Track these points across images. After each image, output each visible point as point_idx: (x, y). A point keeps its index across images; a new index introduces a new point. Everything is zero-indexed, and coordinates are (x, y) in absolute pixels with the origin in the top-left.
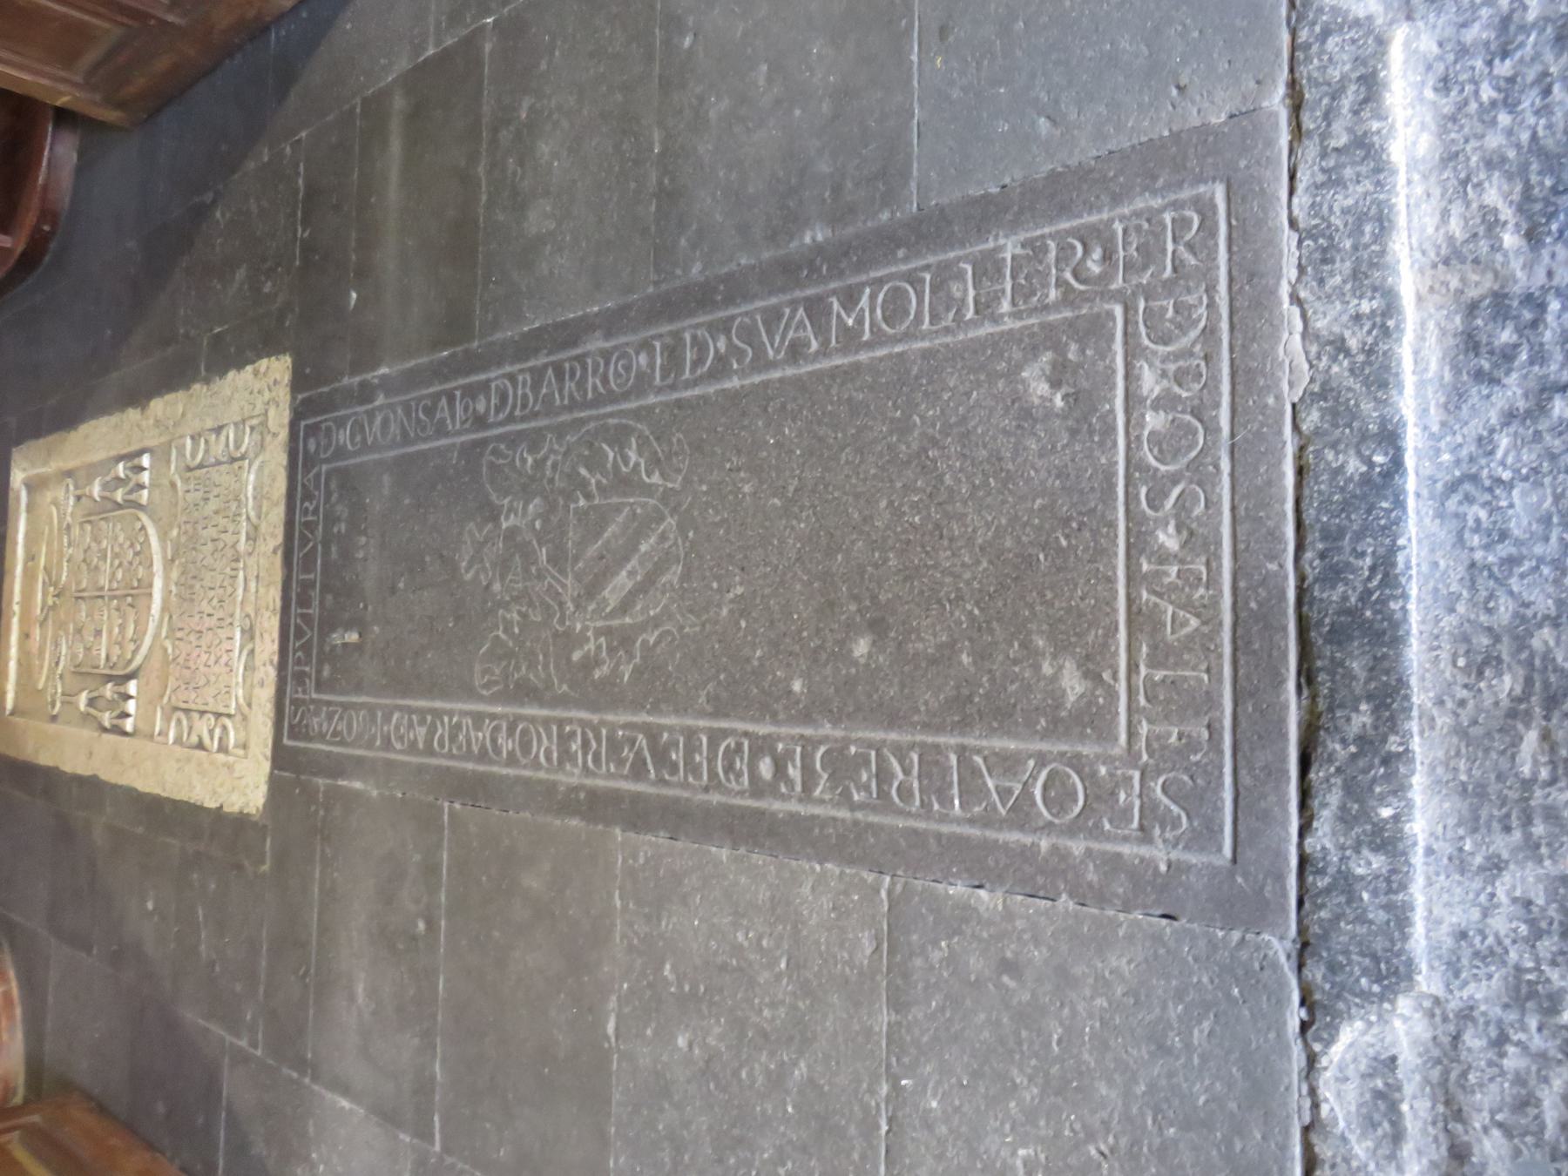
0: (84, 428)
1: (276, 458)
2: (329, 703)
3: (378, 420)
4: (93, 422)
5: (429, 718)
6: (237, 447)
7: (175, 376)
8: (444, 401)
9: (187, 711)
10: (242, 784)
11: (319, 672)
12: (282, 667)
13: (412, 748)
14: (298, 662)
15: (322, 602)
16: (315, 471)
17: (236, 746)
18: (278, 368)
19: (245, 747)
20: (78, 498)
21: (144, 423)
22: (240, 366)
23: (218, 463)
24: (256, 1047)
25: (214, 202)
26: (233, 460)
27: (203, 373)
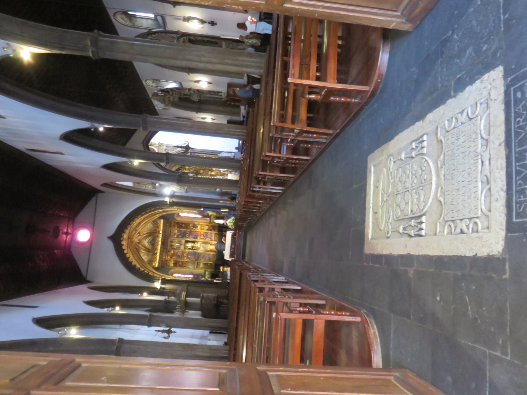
0: (396, 138)
4: (401, 134)
9: (453, 221)
10: (491, 242)
14: (520, 185)
17: (482, 229)
19: (488, 228)
27: (452, 94)
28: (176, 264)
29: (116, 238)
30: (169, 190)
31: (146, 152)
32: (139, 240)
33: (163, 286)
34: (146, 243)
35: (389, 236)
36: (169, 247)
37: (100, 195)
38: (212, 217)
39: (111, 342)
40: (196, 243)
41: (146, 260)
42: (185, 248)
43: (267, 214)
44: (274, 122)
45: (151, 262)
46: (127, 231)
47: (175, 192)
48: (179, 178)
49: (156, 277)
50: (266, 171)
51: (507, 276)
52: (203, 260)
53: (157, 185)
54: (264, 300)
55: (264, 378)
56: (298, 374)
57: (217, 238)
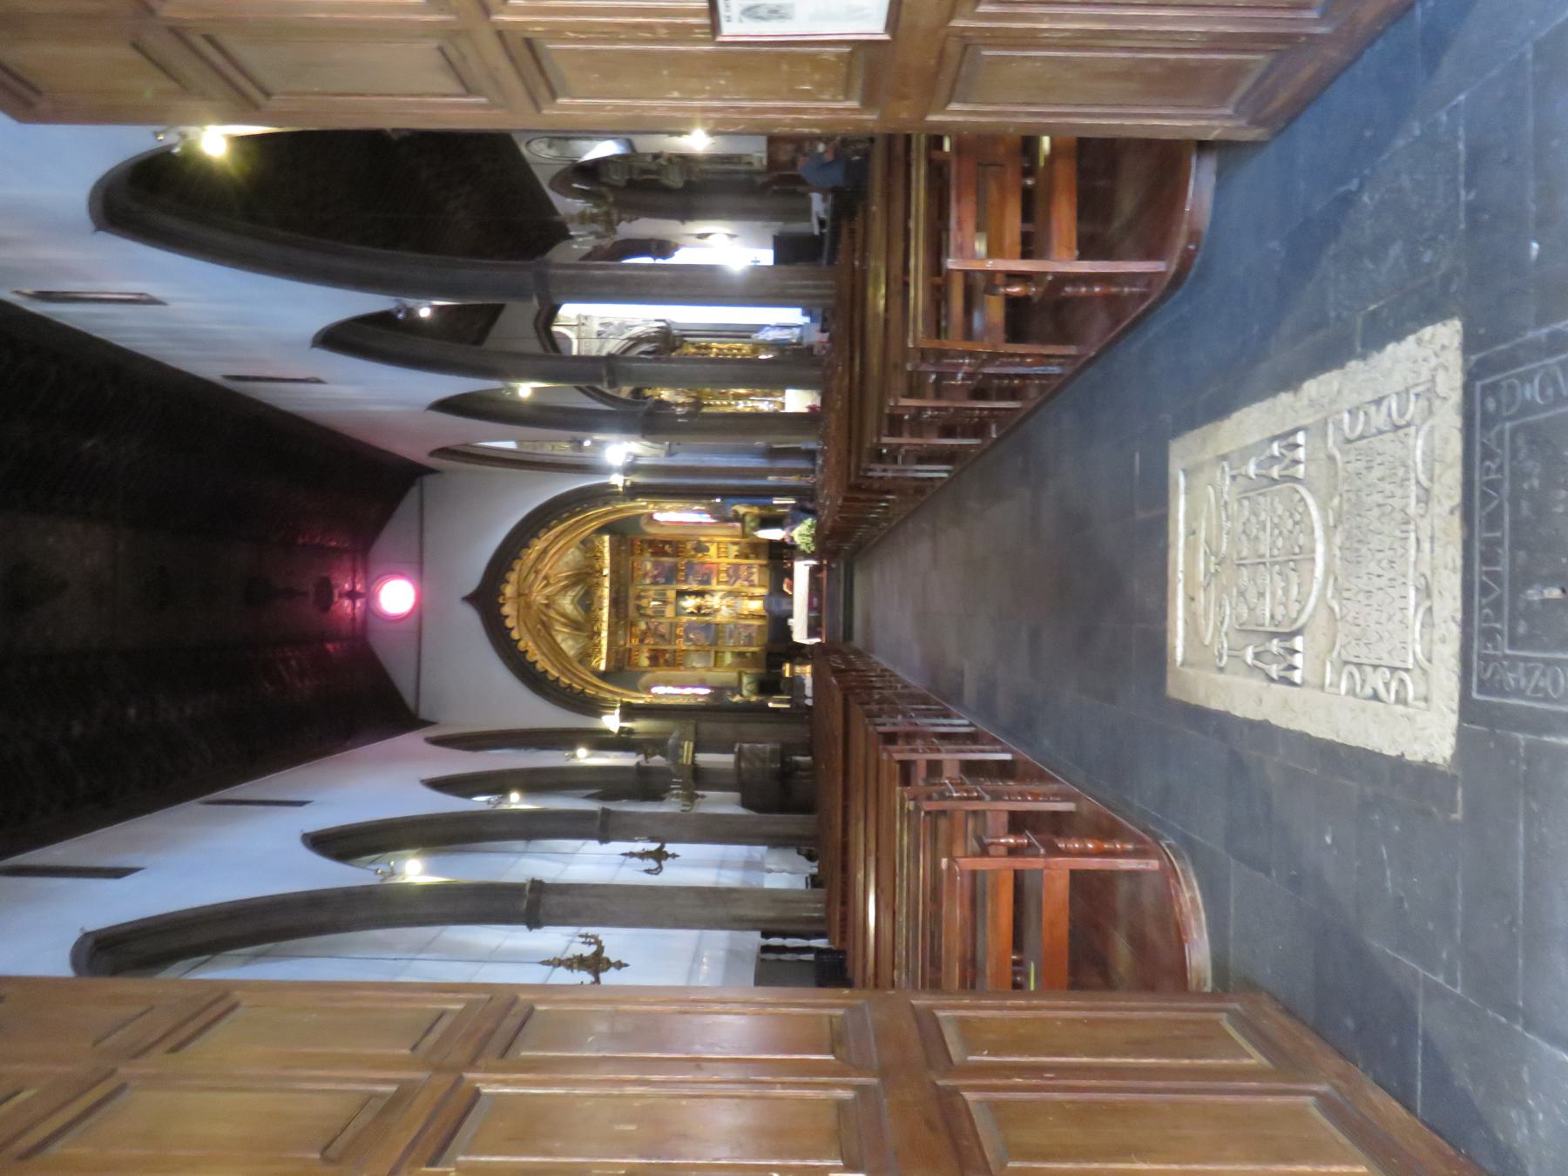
0: (1237, 416)
1: (1449, 420)
2: (1526, 659)
4: (1246, 410)
6: (1401, 415)
7: (1330, 356)
9: (1359, 665)
10: (1427, 732)
11: (1512, 629)
12: (1466, 624)
15: (1513, 560)
16: (1497, 428)
17: (1416, 699)
18: (1446, 335)
19: (1426, 699)
20: (1234, 478)
21: (1298, 405)
22: (1399, 336)
23: (1380, 432)
24: (1455, 986)
25: (1361, 187)
26: (1397, 428)
27: (1359, 349)
28: (655, 658)
29: (486, 599)
30: (619, 453)
31: (551, 357)
32: (547, 598)
33: (627, 725)
34: (567, 603)
35: (1222, 664)
36: (632, 612)
37: (428, 480)
38: (748, 518)
39: (514, 890)
40: (708, 597)
41: (571, 653)
42: (679, 611)
43: (910, 525)
44: (915, 338)
45: (585, 656)
46: (513, 577)
47: (636, 457)
48: (648, 420)
49: (605, 700)
50: (900, 435)
51: (1457, 816)
52: (731, 642)
53: (587, 443)
54: (918, 809)
55: (929, 1028)
56: (1005, 1013)
57: (766, 579)
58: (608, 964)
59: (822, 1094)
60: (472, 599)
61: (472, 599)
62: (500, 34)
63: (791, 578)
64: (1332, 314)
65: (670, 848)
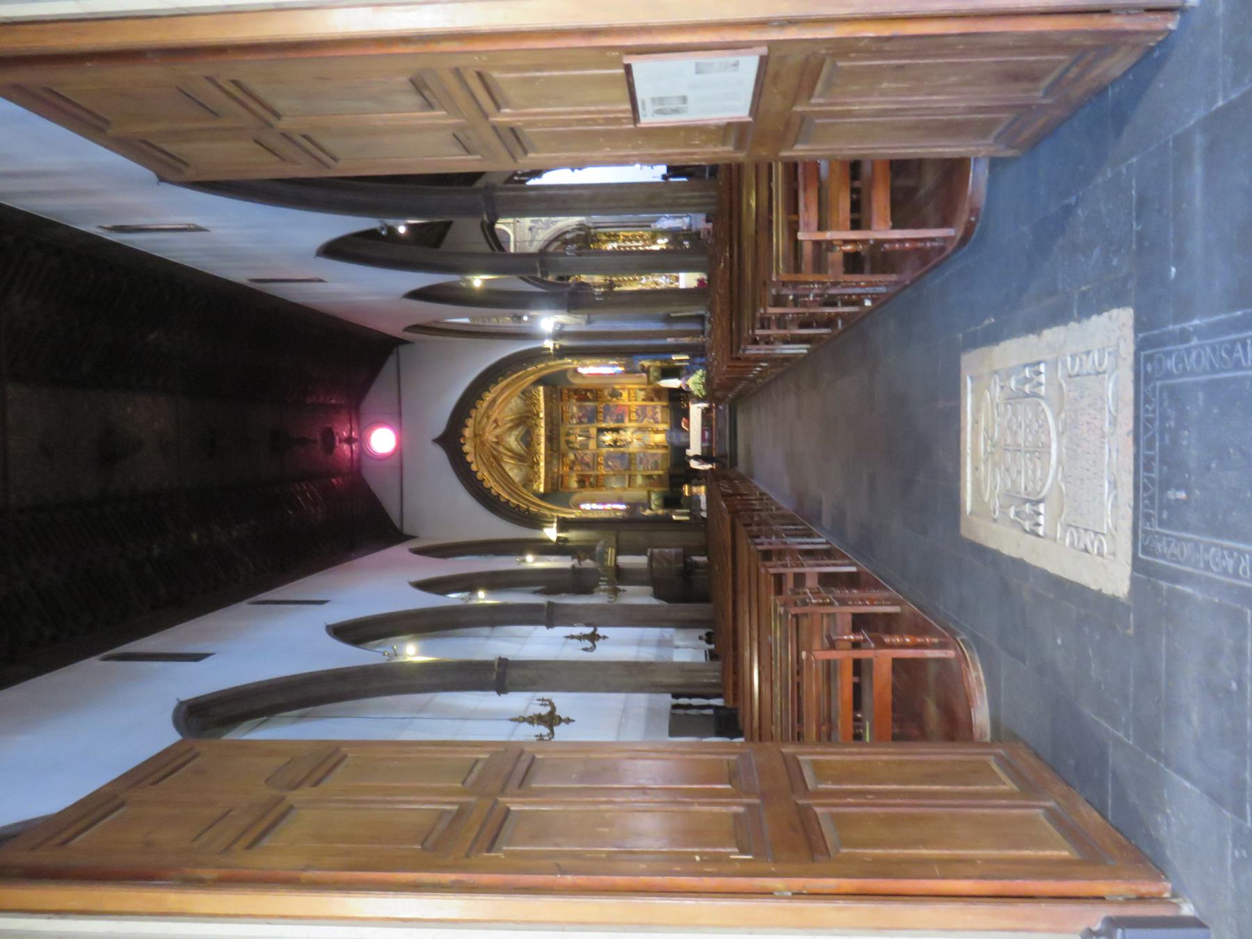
1: (1127, 375)
2: (1167, 536)
3: (1194, 355)
5: (1235, 554)
6: (1101, 365)
7: (1059, 316)
8: (1239, 346)
9: (1077, 528)
10: (1113, 577)
11: (1160, 514)
12: (1136, 508)
13: (1225, 572)
15: (1160, 471)
17: (1109, 553)
18: (1123, 318)
19: (1114, 555)
20: (1002, 387)
22: (1099, 312)
23: (1089, 374)
25: (1077, 203)
26: (1098, 373)
28: (582, 482)
29: (450, 441)
30: (548, 323)
31: (496, 254)
32: (497, 437)
33: (562, 535)
34: (512, 441)
36: (563, 446)
39: (485, 666)
41: (517, 479)
42: (600, 444)
44: (778, 274)
45: (528, 482)
46: (470, 422)
47: (563, 325)
48: (575, 299)
49: (545, 516)
50: (769, 328)
51: (1131, 632)
53: (525, 318)
54: (786, 612)
55: (793, 768)
58: (560, 720)
59: (724, 810)
60: (442, 441)
61: (442, 441)
62: (495, 128)
63: (688, 417)
64: (1060, 287)
65: (601, 631)
